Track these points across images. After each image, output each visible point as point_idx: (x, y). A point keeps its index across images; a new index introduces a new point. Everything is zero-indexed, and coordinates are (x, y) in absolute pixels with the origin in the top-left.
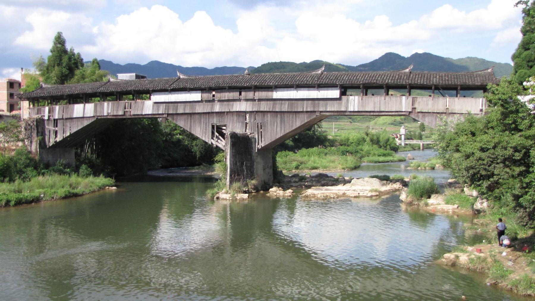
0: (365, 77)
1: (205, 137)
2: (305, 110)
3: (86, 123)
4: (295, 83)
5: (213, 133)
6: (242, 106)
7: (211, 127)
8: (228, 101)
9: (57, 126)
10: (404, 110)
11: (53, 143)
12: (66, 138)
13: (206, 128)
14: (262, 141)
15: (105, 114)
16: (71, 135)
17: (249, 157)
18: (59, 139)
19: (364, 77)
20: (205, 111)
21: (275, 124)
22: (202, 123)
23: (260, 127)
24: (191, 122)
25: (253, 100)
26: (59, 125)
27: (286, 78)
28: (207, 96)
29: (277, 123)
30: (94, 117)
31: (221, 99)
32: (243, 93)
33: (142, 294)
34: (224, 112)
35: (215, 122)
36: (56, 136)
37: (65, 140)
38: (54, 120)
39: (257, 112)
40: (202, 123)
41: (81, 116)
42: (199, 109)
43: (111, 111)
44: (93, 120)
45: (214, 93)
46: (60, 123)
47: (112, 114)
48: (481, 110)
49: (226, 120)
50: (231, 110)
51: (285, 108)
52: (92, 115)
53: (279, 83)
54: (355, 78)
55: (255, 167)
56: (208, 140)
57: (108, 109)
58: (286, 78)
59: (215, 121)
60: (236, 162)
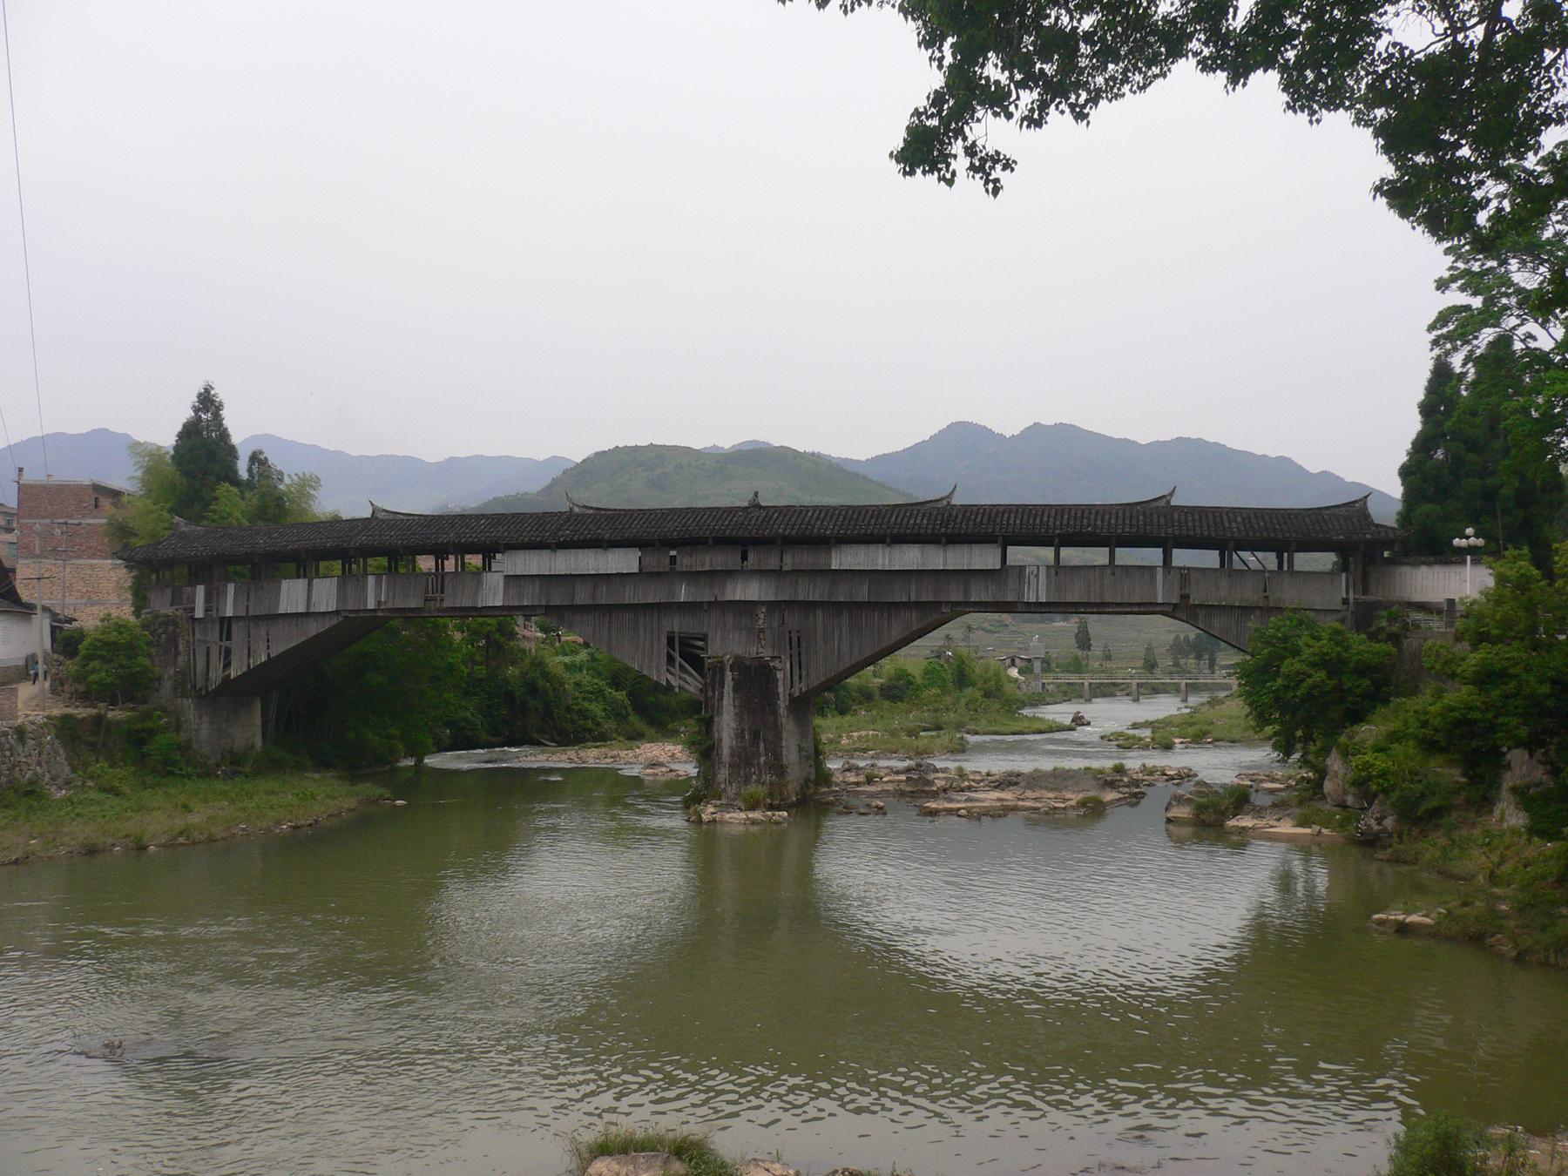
0: (1062, 517)
1: (650, 668)
2: (913, 600)
3: (313, 629)
4: (889, 531)
5: (671, 660)
6: (749, 591)
7: (664, 641)
8: (712, 574)
9: (229, 638)
10: (1160, 600)
11: (219, 681)
12: (255, 668)
13: (652, 647)
14: (800, 678)
15: (371, 605)
16: (270, 660)
17: (771, 719)
18: (233, 673)
19: (1059, 517)
20: (650, 600)
21: (837, 634)
22: (642, 632)
23: (797, 646)
24: (610, 628)
25: (778, 573)
26: (234, 634)
27: (861, 519)
28: (658, 562)
29: (841, 631)
30: (337, 612)
31: (693, 569)
32: (752, 556)
33: (1178, 784)
34: (702, 603)
35: (676, 629)
36: (227, 665)
37: (250, 675)
38: (223, 620)
39: (788, 603)
40: (642, 632)
41: (302, 609)
42: (630, 595)
43: (388, 597)
44: (335, 622)
45: (673, 553)
46: (238, 631)
47: (390, 605)
48: (1345, 601)
49: (706, 622)
50: (720, 599)
51: (863, 593)
52: (332, 607)
53: (849, 532)
54: (1038, 521)
55: (784, 744)
56: (659, 676)
57: (378, 594)
58: (861, 519)
59: (677, 624)
60: (743, 731)
